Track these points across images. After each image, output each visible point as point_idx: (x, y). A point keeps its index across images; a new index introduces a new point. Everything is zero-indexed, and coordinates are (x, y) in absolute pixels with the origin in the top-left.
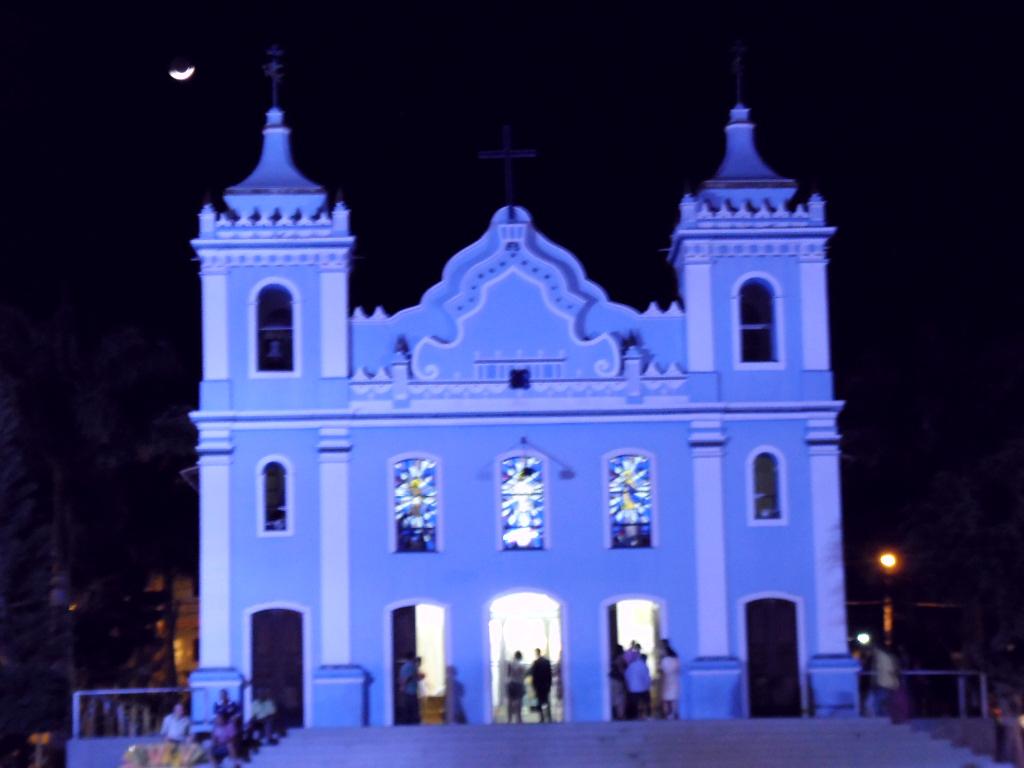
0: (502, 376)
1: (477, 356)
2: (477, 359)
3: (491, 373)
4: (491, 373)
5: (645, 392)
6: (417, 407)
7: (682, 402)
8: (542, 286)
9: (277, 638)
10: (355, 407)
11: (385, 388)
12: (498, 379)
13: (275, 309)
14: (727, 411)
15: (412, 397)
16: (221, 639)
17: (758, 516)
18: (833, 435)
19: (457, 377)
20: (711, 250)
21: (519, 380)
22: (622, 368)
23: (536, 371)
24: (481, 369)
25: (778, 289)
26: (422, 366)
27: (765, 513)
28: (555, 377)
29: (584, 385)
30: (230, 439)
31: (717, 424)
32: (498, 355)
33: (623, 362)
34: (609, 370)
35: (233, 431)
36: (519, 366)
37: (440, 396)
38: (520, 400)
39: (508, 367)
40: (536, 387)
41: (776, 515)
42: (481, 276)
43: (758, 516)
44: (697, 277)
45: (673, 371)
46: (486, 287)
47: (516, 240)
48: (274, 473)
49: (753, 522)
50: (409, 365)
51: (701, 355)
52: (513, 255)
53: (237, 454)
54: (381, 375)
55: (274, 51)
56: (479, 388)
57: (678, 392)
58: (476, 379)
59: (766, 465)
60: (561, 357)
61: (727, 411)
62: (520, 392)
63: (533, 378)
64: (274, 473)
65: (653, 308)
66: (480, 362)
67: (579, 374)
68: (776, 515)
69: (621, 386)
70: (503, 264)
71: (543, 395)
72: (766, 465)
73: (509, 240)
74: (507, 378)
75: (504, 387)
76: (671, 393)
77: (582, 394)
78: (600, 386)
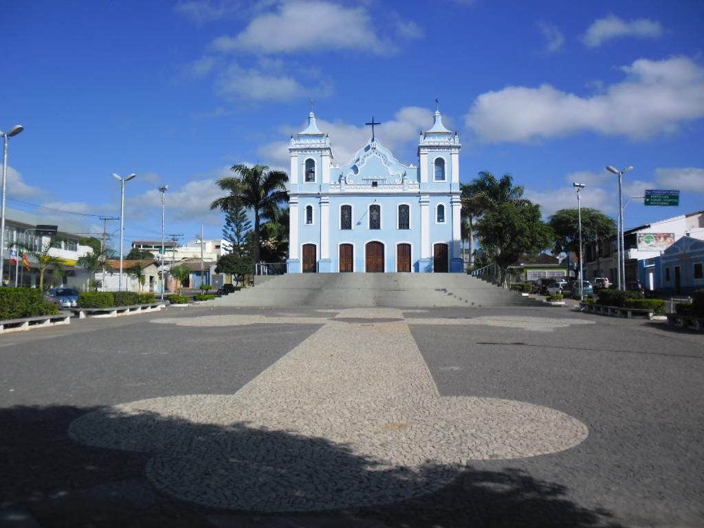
6: (347, 191)
9: (310, 251)
10: (331, 191)
13: (310, 163)
16: (295, 252)
18: (459, 200)
21: (375, 184)
22: (403, 182)
26: (349, 179)
32: (370, 178)
39: (371, 181)
44: (424, 159)
45: (416, 182)
49: (437, 223)
51: (424, 178)
54: (338, 183)
55: (311, 113)
59: (441, 208)
62: (375, 187)
65: (411, 166)
71: (382, 188)
72: (441, 208)
75: (370, 186)
77: (392, 188)
78: (397, 186)
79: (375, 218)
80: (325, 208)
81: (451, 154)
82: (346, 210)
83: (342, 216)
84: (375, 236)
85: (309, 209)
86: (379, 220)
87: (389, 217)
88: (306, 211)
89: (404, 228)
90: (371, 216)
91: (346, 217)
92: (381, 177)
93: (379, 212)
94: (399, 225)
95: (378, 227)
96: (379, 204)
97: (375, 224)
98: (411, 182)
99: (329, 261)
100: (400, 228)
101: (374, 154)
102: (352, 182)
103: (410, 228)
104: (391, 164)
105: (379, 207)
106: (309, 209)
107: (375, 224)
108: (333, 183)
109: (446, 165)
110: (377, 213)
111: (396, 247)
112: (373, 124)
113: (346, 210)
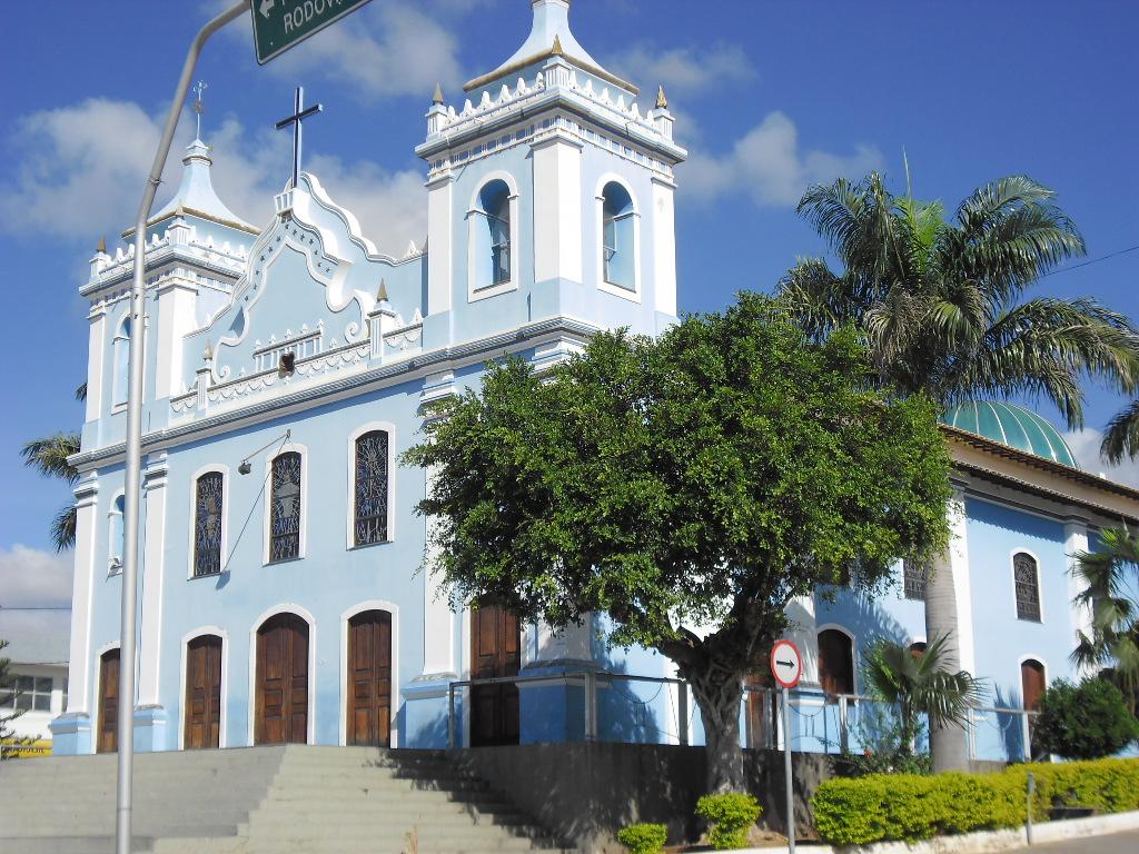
0: (275, 364)
1: (259, 345)
2: (258, 349)
4: (267, 364)
7: (416, 352)
10: (174, 423)
11: (193, 399)
12: (272, 367)
19: (245, 373)
21: (288, 364)
23: (301, 353)
25: (514, 191)
28: (315, 354)
33: (368, 322)
36: (286, 352)
40: (299, 369)
42: (263, 259)
45: (417, 318)
46: (265, 272)
47: (288, 207)
56: (254, 384)
58: (257, 372)
67: (336, 343)
73: (284, 209)
75: (277, 373)
78: (353, 351)
80: (159, 500)
81: (531, 155)
83: (198, 519)
84: (284, 593)
85: (121, 503)
90: (276, 501)
91: (211, 519)
92: (306, 329)
94: (358, 523)
97: (285, 544)
98: (400, 323)
99: (144, 719)
100: (361, 542)
101: (288, 239)
104: (335, 262)
105: (297, 456)
106: (121, 503)
107: (285, 544)
108: (186, 392)
109: (514, 206)
110: (297, 487)
111: (345, 625)
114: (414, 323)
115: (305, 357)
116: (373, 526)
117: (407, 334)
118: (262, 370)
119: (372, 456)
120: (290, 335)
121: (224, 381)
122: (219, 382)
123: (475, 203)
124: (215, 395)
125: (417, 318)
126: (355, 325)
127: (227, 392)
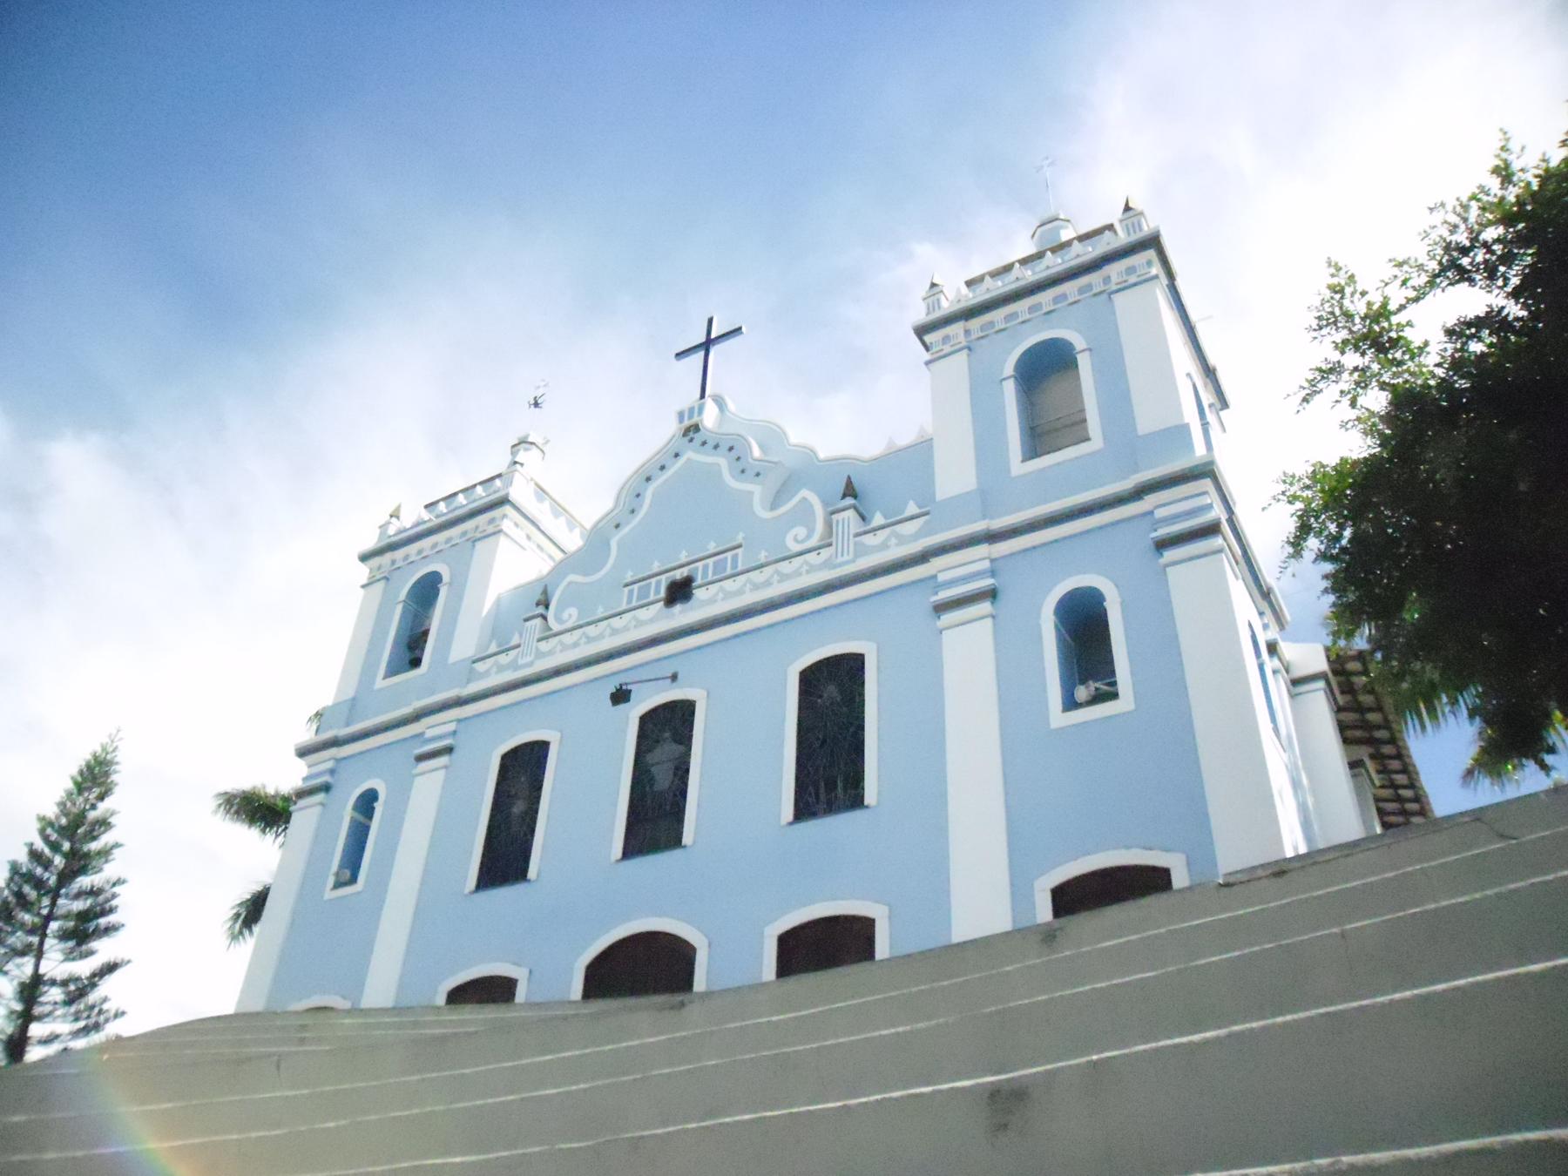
0: (657, 592)
1: (629, 577)
2: (629, 579)
3: (644, 593)
4: (644, 593)
5: (861, 551)
8: (722, 461)
11: (513, 653)
12: (652, 597)
14: (992, 537)
15: (540, 655)
17: (1071, 704)
19: (601, 612)
20: (967, 332)
21: (679, 591)
24: (631, 592)
27: (1082, 693)
29: (768, 570)
30: (332, 772)
31: (986, 564)
32: (656, 567)
33: (829, 525)
34: (808, 537)
35: (338, 761)
36: (678, 575)
37: (576, 645)
38: (683, 615)
39: (664, 581)
40: (699, 594)
41: (1114, 696)
42: (648, 479)
43: (1071, 704)
47: (695, 419)
48: (367, 802)
49: (1058, 718)
50: (545, 618)
52: (691, 440)
53: (333, 792)
57: (916, 537)
58: (624, 607)
60: (740, 538)
61: (992, 537)
62: (678, 608)
63: (699, 581)
64: (367, 802)
66: (627, 585)
67: (763, 557)
68: (1114, 696)
69: (825, 553)
70: (677, 455)
71: (712, 601)
74: (663, 594)
76: (902, 540)
78: (797, 561)
79: (663, 778)
82: (524, 769)
86: (683, 794)
87: (745, 756)
88: (347, 814)
89: (832, 808)
91: (518, 808)
93: (685, 738)
95: (673, 840)
96: (690, 697)
97: (655, 819)
100: (805, 808)
101: (691, 455)
102: (572, 615)
103: (870, 795)
107: (655, 819)
108: (493, 648)
109: (1084, 363)
110: (682, 748)
112: (707, 345)
113: (524, 769)
114: (908, 513)
115: (710, 578)
116: (831, 786)
117: (898, 528)
118: (634, 604)
119: (831, 691)
120: (683, 558)
121: (569, 625)
122: (555, 626)
123: (1009, 368)
124: (544, 646)
125: (912, 509)
126: (801, 532)
127: (568, 639)
